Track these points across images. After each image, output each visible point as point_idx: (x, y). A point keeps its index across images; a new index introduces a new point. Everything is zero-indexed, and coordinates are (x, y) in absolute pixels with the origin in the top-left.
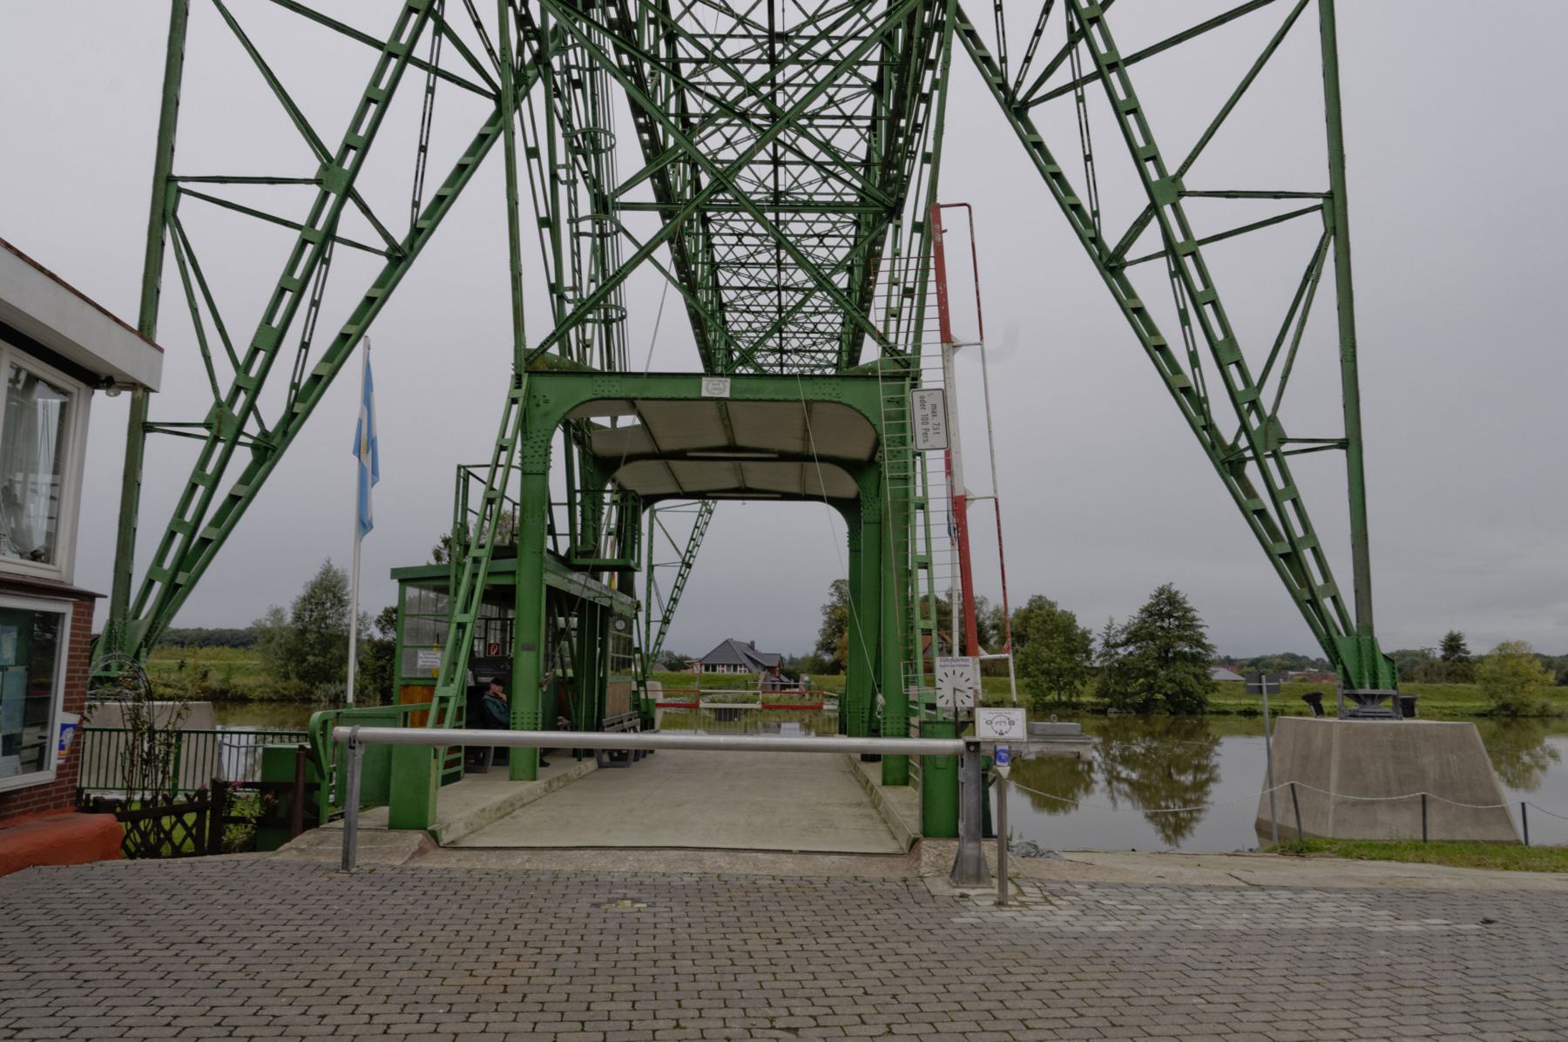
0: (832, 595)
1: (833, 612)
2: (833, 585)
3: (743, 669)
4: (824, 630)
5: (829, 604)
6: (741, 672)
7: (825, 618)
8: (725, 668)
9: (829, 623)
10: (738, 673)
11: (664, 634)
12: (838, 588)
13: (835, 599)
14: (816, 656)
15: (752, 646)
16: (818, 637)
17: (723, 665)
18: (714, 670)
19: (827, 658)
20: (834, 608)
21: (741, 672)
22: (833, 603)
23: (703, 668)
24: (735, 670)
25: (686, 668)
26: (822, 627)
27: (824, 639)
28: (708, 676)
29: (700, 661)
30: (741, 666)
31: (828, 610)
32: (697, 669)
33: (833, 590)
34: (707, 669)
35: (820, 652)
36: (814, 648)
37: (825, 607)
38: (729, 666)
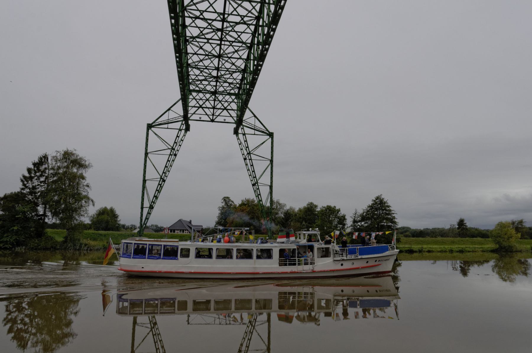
0: (222, 203)
1: (223, 209)
2: (223, 199)
3: (187, 231)
4: (219, 216)
5: (221, 206)
6: (186, 233)
7: (219, 212)
8: (179, 231)
9: (222, 214)
10: (185, 233)
11: (148, 219)
12: (225, 200)
13: (223, 204)
14: (215, 226)
15: (190, 222)
16: (217, 219)
17: (178, 230)
18: (174, 232)
19: (221, 228)
20: (223, 208)
21: (186, 233)
22: (223, 206)
23: (169, 231)
24: (183, 232)
25: (162, 231)
26: (218, 215)
27: (219, 220)
28: (172, 234)
29: (168, 228)
30: (186, 230)
31: (221, 209)
32: (166, 232)
33: (223, 201)
34: (171, 232)
35: (217, 225)
36: (215, 224)
37: (219, 207)
38: (180, 230)
